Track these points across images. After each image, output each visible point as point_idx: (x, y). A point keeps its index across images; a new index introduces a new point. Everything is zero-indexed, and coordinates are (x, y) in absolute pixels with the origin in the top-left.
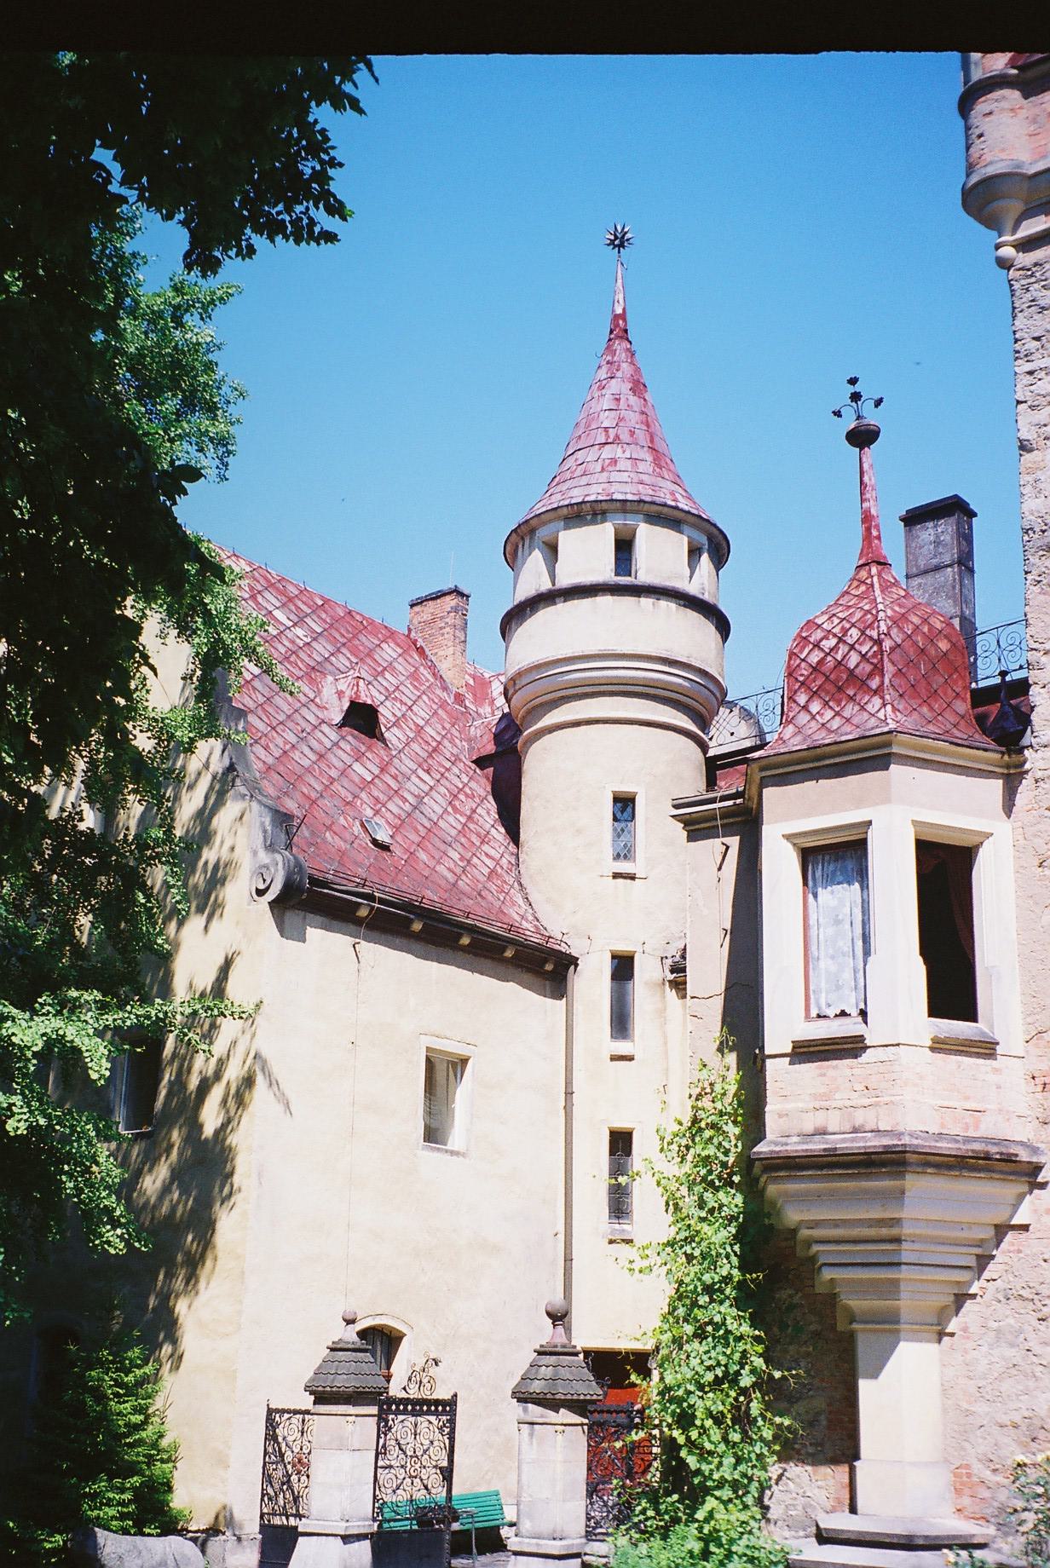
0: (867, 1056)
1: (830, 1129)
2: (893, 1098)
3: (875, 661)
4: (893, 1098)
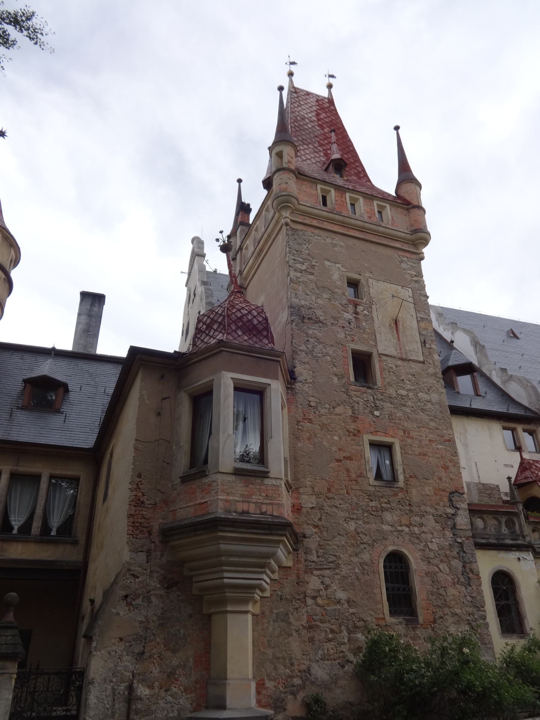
0: (267, 481)
1: (250, 512)
2: (280, 502)
3: (265, 325)
4: (280, 502)
